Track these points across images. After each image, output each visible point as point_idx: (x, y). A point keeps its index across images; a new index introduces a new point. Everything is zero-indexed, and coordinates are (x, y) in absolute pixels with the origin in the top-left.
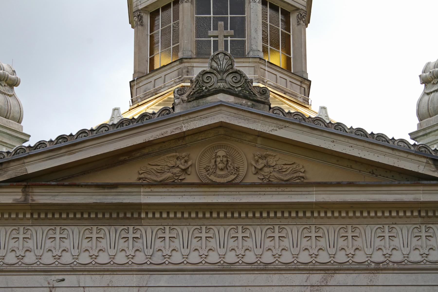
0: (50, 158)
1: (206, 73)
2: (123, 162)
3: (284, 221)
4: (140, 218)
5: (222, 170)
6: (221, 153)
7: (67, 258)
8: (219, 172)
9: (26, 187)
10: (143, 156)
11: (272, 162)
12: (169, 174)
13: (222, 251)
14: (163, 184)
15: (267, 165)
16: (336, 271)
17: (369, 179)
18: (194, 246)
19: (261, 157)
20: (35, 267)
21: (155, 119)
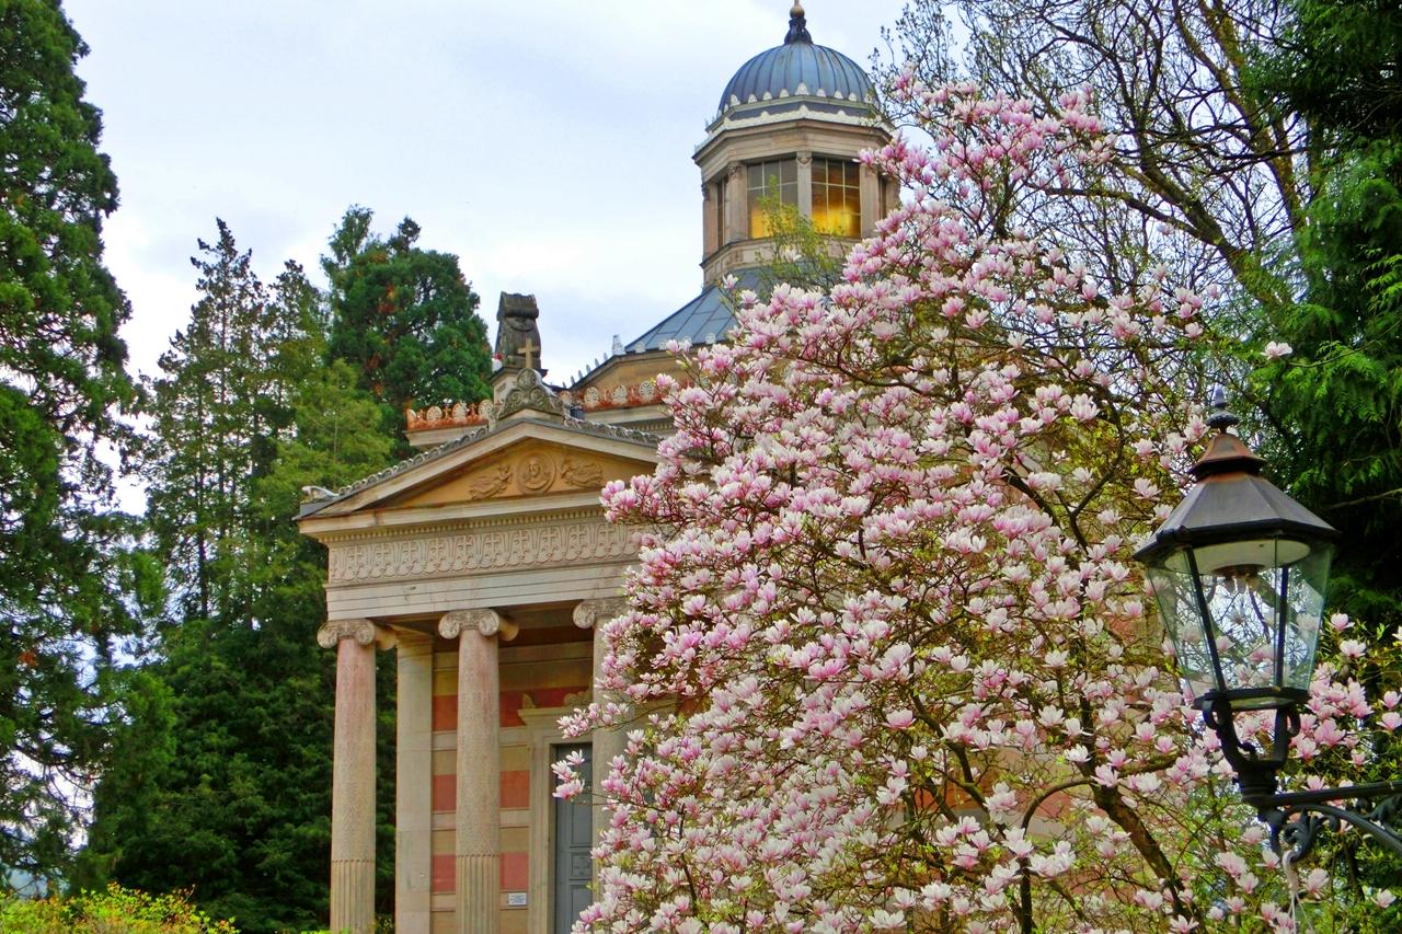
1: (514, 390)
2: (459, 477)
6: (533, 462)
10: (474, 470)
11: (574, 465)
12: (492, 486)
13: (535, 552)
15: (571, 469)
19: (566, 462)
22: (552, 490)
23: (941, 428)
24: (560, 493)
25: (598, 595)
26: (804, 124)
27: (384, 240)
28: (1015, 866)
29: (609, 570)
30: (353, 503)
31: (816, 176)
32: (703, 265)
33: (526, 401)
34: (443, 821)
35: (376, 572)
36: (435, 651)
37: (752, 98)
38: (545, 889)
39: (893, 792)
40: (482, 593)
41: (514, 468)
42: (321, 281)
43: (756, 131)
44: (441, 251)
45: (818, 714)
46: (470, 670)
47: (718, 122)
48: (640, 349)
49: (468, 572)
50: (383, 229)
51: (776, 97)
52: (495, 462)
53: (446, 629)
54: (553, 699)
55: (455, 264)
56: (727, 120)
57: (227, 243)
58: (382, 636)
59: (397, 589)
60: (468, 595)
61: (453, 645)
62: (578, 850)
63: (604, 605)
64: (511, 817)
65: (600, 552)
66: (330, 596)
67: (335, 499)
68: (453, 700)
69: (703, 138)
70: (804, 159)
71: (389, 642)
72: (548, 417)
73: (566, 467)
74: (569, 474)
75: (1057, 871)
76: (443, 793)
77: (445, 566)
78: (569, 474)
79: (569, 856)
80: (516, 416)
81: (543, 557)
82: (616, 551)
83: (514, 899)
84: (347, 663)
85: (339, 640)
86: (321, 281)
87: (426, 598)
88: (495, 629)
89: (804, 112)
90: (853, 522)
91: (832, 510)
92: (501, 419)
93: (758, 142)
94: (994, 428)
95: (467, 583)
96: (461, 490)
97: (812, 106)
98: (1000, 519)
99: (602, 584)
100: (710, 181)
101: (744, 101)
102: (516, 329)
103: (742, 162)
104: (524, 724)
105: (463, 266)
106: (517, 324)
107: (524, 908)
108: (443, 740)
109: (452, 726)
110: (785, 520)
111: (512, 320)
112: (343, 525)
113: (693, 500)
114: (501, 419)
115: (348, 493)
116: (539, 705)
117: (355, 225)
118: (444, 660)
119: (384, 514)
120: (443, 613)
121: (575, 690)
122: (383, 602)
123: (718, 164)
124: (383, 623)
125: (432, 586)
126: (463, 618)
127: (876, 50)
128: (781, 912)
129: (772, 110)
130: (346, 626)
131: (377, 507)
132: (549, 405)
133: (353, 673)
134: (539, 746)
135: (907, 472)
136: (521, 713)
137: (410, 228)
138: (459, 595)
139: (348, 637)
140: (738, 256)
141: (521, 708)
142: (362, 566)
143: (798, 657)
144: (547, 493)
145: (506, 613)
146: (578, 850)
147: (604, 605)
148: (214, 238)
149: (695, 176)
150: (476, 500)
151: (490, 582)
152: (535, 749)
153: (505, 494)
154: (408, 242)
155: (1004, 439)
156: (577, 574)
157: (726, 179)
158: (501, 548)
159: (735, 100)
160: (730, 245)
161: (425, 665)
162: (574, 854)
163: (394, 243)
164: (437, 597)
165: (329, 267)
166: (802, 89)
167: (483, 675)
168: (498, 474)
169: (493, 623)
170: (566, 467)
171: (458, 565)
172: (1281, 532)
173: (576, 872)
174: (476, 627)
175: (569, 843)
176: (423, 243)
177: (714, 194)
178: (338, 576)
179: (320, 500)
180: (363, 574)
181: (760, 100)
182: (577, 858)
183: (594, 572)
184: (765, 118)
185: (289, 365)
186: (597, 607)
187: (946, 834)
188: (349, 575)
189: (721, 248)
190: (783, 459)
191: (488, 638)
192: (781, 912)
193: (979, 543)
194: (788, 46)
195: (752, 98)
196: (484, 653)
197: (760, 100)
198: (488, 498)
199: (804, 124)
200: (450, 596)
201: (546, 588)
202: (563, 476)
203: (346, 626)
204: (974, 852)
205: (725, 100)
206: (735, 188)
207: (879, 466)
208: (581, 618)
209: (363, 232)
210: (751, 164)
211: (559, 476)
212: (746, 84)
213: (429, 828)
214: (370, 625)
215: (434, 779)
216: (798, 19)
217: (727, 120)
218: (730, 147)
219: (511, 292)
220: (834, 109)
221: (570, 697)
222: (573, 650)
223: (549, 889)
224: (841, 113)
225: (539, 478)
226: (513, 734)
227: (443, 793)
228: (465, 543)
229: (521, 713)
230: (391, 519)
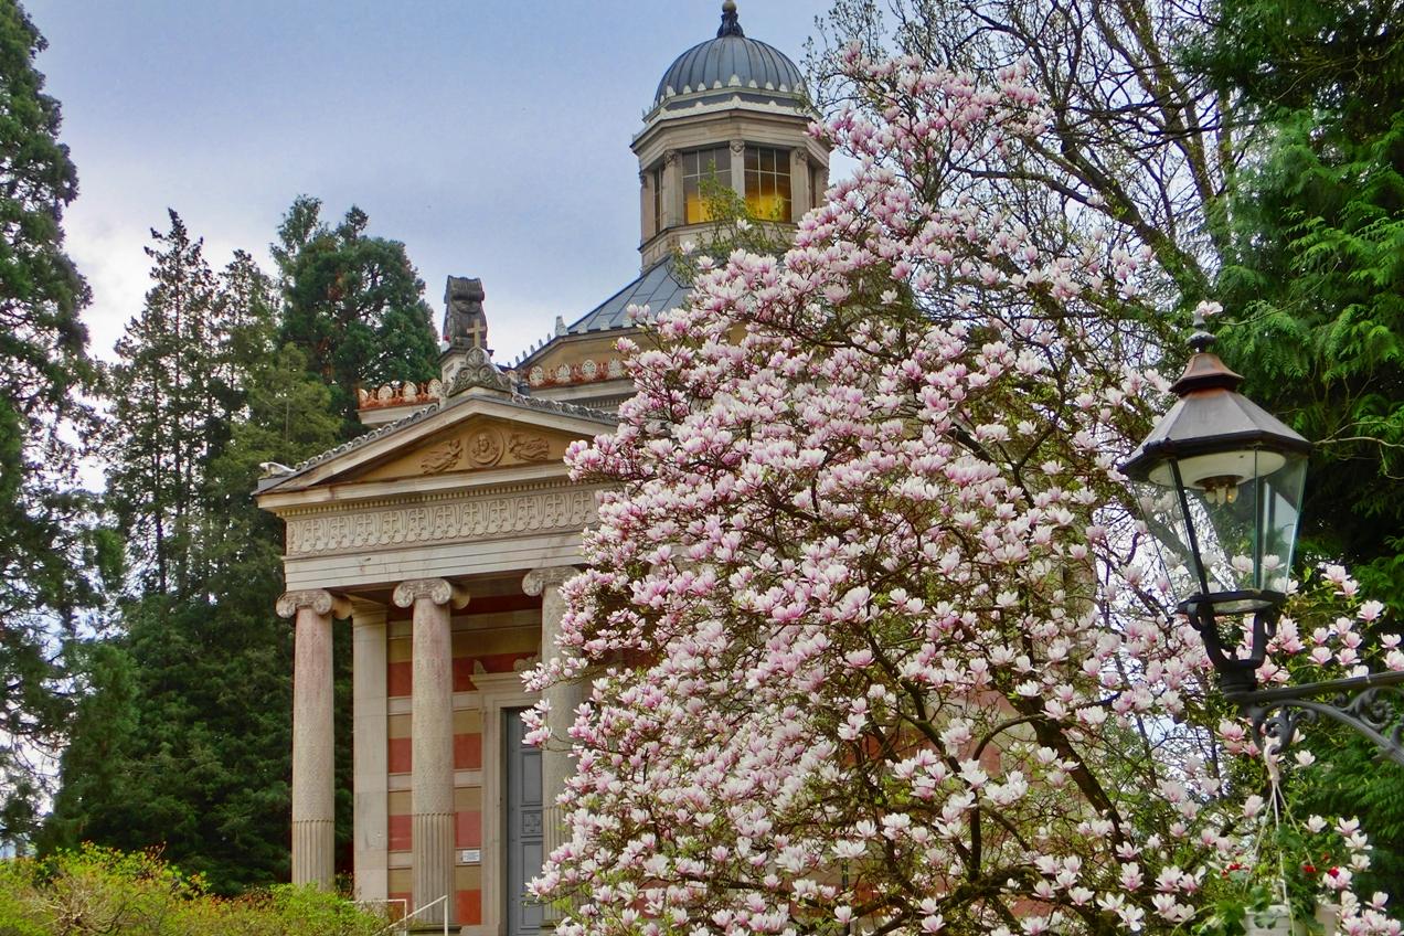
3: (530, 493)
6: (482, 437)
7: (372, 540)
10: (424, 446)
11: (522, 440)
15: (518, 444)
19: (514, 437)
22: (503, 463)
23: (892, 385)
24: (508, 467)
26: (735, 114)
27: (333, 228)
28: (971, 796)
29: (556, 541)
30: (308, 479)
31: (749, 164)
32: (641, 249)
33: (475, 379)
34: (399, 782)
36: (389, 620)
37: (687, 90)
38: (497, 845)
39: (854, 728)
40: (434, 564)
41: (464, 444)
42: (271, 269)
44: (387, 239)
45: (782, 655)
47: (656, 112)
48: (582, 329)
49: (420, 544)
50: (330, 219)
52: (444, 439)
53: (401, 599)
54: (502, 664)
55: (402, 251)
56: (663, 110)
57: (179, 233)
58: (338, 607)
59: (352, 561)
60: (421, 565)
61: (408, 613)
62: (527, 809)
63: (552, 574)
64: (463, 778)
65: (548, 523)
66: (288, 568)
67: (292, 475)
68: (407, 667)
69: (641, 127)
70: (737, 148)
71: (346, 612)
72: (496, 394)
73: (514, 442)
75: (1011, 799)
76: (398, 756)
77: (398, 538)
79: (520, 815)
80: (465, 394)
81: (493, 528)
82: (563, 522)
83: (470, 856)
85: (297, 610)
86: (271, 269)
87: (381, 569)
88: (448, 598)
89: (736, 103)
90: (809, 475)
91: (791, 462)
93: (692, 131)
94: (943, 383)
95: (420, 554)
96: (413, 465)
97: (745, 97)
98: (950, 468)
99: (549, 553)
100: (647, 169)
101: (679, 92)
102: (462, 311)
103: (678, 150)
104: (476, 689)
105: (409, 253)
106: (464, 307)
107: (477, 865)
108: (398, 705)
110: (747, 472)
111: (459, 303)
113: (658, 455)
115: (304, 469)
116: (490, 670)
117: (302, 217)
118: (399, 629)
119: (340, 489)
120: (397, 583)
121: (524, 656)
122: (340, 573)
123: (655, 152)
124: (339, 594)
125: (386, 558)
126: (416, 587)
127: (810, 39)
128: (743, 847)
129: (706, 100)
130: (304, 597)
131: (332, 482)
133: (311, 639)
134: (490, 710)
135: (859, 427)
136: (472, 678)
137: (357, 217)
138: (414, 566)
139: (306, 607)
140: (675, 241)
142: (319, 539)
143: (761, 602)
144: (495, 467)
145: (457, 582)
146: (527, 809)
147: (552, 574)
148: (166, 228)
149: (633, 164)
150: (427, 475)
151: (442, 552)
153: (456, 468)
154: (355, 231)
155: (953, 394)
156: (525, 544)
157: (663, 167)
158: (452, 520)
159: (670, 91)
160: (667, 230)
161: (380, 635)
163: (343, 231)
165: (279, 255)
166: (735, 81)
167: (436, 641)
168: (449, 449)
169: (444, 593)
170: (514, 442)
171: (411, 537)
172: (1260, 443)
173: (527, 829)
174: (428, 596)
175: (520, 802)
176: (370, 232)
177: (651, 180)
178: (295, 549)
179: (277, 476)
180: (320, 546)
181: (694, 91)
183: (543, 542)
184: (700, 108)
185: (243, 348)
186: (545, 576)
187: (903, 768)
188: (306, 548)
189: (658, 233)
190: (742, 415)
191: (441, 607)
192: (743, 847)
193: (933, 491)
194: (720, 40)
195: (687, 90)
197: (694, 91)
198: (440, 472)
199: (735, 114)
200: (405, 567)
201: (497, 558)
202: (512, 450)
203: (304, 597)
204: (932, 783)
205: (661, 92)
206: (671, 176)
207: (833, 421)
208: (530, 587)
209: (310, 221)
211: (508, 450)
212: (682, 76)
213: (385, 789)
214: (328, 596)
215: (390, 742)
216: (730, 14)
217: (663, 110)
218: (665, 137)
219: (457, 275)
220: (765, 99)
221: (519, 663)
222: (521, 617)
223: (501, 848)
224: (772, 103)
226: (464, 699)
227: (398, 756)
228: (417, 516)
229: (472, 678)
230: (345, 493)
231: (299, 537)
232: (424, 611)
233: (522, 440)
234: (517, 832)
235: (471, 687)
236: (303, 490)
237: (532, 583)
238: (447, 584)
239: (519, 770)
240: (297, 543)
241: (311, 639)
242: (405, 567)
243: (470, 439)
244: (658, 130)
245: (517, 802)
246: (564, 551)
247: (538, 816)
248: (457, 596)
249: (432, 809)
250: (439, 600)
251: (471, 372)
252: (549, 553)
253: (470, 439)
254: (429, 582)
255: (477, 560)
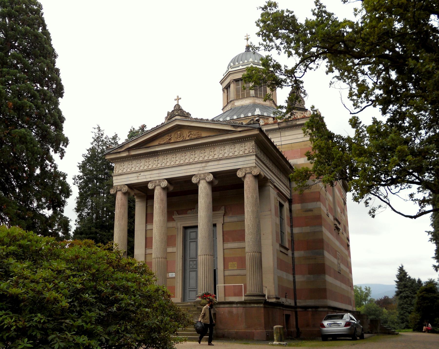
0: (134, 142)
4: (158, 154)
5: (179, 137)
6: (179, 133)
8: (179, 138)
9: (128, 151)
14: (164, 144)
15: (191, 134)
16: (209, 162)
17: (218, 134)
18: (210, 154)
19: (189, 132)
20: (143, 170)
21: (160, 126)
25: (200, 172)
29: (203, 165)
33: (177, 114)
34: (148, 251)
35: (129, 170)
36: (147, 200)
37: (237, 63)
38: (181, 271)
41: (173, 136)
43: (238, 71)
46: (158, 199)
49: (157, 168)
51: (243, 63)
60: (157, 175)
62: (190, 260)
63: (202, 175)
65: (201, 159)
68: (152, 214)
72: (184, 118)
73: (190, 133)
74: (190, 135)
76: (148, 243)
78: (190, 135)
81: (182, 162)
82: (206, 158)
84: (119, 199)
88: (166, 185)
92: (169, 120)
96: (156, 143)
99: (201, 169)
103: (234, 80)
104: (174, 220)
107: (174, 278)
109: (152, 222)
112: (118, 156)
114: (169, 120)
116: (179, 214)
122: (131, 179)
124: (130, 186)
126: (156, 183)
129: (242, 66)
130: (119, 187)
132: (184, 114)
133: (120, 199)
134: (179, 227)
136: (173, 217)
139: (119, 191)
141: (173, 215)
145: (169, 180)
146: (190, 260)
147: (202, 175)
149: (221, 87)
151: (164, 171)
152: (178, 228)
156: (193, 166)
159: (232, 64)
160: (231, 101)
161: (144, 204)
162: (190, 261)
164: (148, 177)
167: (162, 200)
169: (165, 184)
170: (190, 133)
171: (154, 166)
174: (160, 185)
177: (226, 91)
180: (125, 171)
181: (239, 64)
182: (191, 262)
183: (199, 165)
184: (241, 67)
186: (200, 176)
188: (120, 172)
189: (228, 103)
196: (162, 194)
200: (152, 176)
201: (183, 171)
202: (189, 136)
203: (119, 187)
205: (229, 65)
210: (237, 81)
211: (187, 136)
214: (126, 186)
225: (181, 138)
226: (171, 224)
227: (148, 243)
230: (133, 153)
231: (118, 168)
232: (158, 190)
233: (192, 133)
234: (188, 267)
235: (173, 220)
236: (119, 152)
237: (195, 179)
238: (165, 180)
239: (188, 250)
240: (117, 170)
241: (120, 199)
242: (152, 176)
243: (175, 134)
244: (229, 74)
245: (188, 258)
246: (206, 168)
247: (195, 262)
248: (169, 185)
249: (159, 256)
250: (163, 186)
251: (175, 112)
252: (201, 169)
253: (175, 134)
254: (160, 181)
255: (177, 172)
